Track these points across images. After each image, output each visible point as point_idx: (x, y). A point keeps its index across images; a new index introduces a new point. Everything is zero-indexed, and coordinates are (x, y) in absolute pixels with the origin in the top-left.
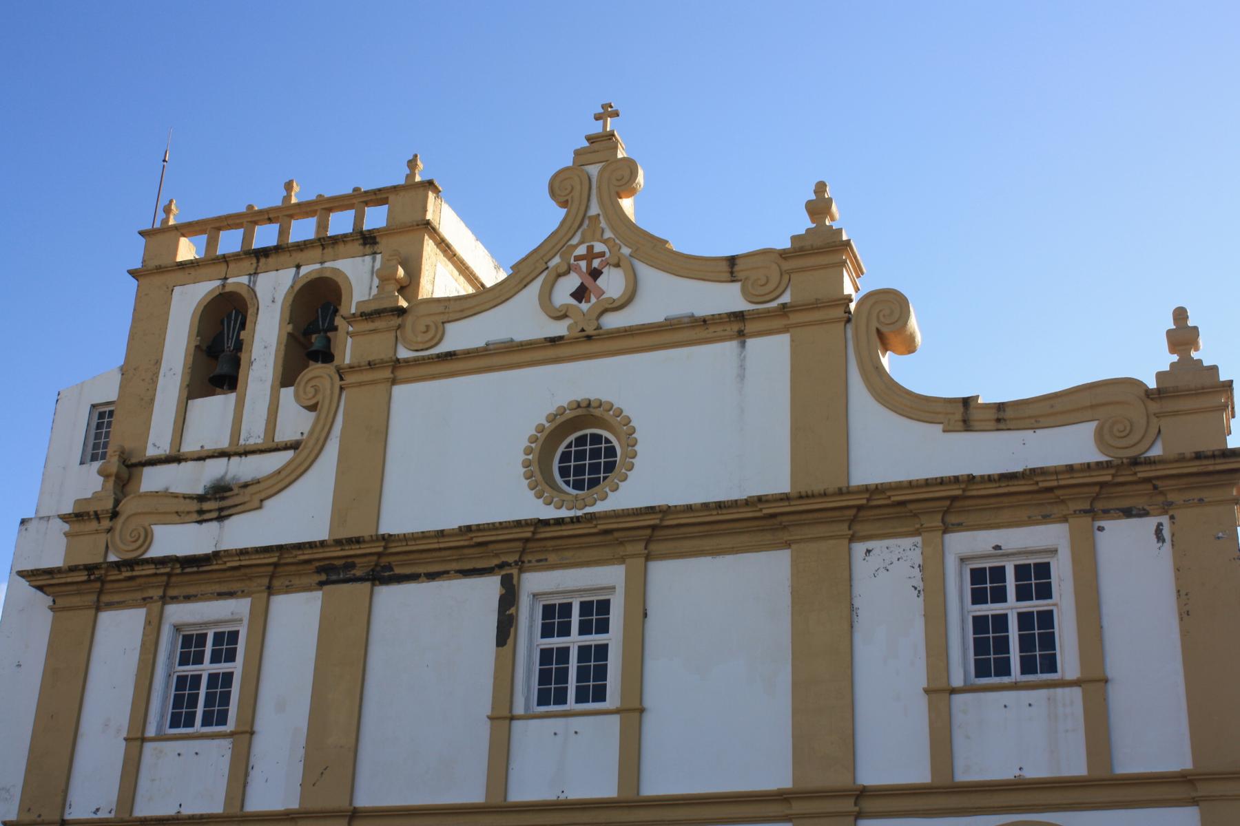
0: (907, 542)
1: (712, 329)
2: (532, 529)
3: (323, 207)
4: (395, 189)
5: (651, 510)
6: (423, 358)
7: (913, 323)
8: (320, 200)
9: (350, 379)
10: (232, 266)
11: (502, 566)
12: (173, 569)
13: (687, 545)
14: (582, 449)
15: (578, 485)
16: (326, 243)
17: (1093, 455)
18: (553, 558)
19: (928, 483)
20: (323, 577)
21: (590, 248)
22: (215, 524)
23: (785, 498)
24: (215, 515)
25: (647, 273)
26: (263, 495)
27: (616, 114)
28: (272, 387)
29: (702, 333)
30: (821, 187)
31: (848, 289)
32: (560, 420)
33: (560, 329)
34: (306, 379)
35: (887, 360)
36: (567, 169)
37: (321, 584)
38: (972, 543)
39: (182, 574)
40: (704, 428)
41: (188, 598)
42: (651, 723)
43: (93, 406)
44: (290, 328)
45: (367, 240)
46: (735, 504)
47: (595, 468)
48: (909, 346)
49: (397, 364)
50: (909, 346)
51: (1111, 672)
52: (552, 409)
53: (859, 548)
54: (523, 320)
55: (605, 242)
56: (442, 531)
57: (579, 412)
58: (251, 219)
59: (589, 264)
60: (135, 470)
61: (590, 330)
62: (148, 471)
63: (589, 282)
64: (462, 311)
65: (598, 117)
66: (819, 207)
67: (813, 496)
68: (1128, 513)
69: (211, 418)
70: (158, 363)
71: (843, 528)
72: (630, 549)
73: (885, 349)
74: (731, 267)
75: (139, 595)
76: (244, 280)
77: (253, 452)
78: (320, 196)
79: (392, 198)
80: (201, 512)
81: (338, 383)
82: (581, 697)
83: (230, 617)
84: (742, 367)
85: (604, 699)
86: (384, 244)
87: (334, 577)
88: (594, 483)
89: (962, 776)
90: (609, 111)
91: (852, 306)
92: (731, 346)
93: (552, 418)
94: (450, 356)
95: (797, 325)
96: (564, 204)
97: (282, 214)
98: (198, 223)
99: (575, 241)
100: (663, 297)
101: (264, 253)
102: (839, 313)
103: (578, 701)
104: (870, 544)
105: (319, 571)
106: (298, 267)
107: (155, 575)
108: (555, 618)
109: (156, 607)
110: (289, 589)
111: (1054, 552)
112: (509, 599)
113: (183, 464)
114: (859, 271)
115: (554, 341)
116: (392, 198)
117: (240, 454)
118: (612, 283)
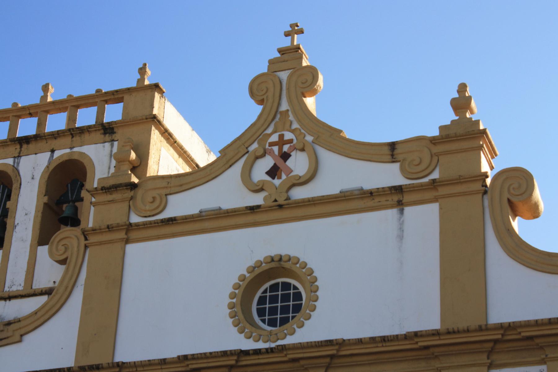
1: (377, 200)
2: (235, 358)
3: (72, 105)
4: (129, 90)
5: (329, 343)
6: (151, 223)
7: (537, 194)
9: (93, 239)
15: (272, 323)
16: (74, 133)
21: (281, 136)
23: (435, 333)
25: (325, 155)
26: (22, 331)
27: (301, 32)
29: (369, 203)
30: (462, 88)
31: (485, 167)
32: (257, 271)
33: (258, 199)
34: (57, 240)
35: (516, 224)
36: (263, 75)
44: (46, 199)
45: (107, 130)
46: (396, 338)
47: (285, 310)
48: (534, 212)
49: (130, 227)
50: (534, 212)
52: (251, 263)
54: (228, 192)
55: (293, 131)
56: (164, 360)
57: (273, 265)
59: (280, 149)
61: (281, 201)
63: (280, 162)
64: (181, 185)
65: (287, 34)
66: (461, 104)
67: (459, 332)
71: (483, 358)
73: (515, 215)
74: (392, 151)
77: (16, 297)
78: (70, 96)
79: (126, 97)
81: (83, 242)
84: (401, 229)
86: (119, 134)
88: (285, 321)
90: (295, 30)
91: (488, 181)
92: (392, 213)
94: (171, 221)
96: (260, 102)
97: (40, 110)
99: (269, 131)
100: (339, 175)
101: (26, 140)
102: (477, 186)
106: (53, 151)
114: (493, 153)
115: (253, 209)
116: (126, 97)
118: (298, 164)
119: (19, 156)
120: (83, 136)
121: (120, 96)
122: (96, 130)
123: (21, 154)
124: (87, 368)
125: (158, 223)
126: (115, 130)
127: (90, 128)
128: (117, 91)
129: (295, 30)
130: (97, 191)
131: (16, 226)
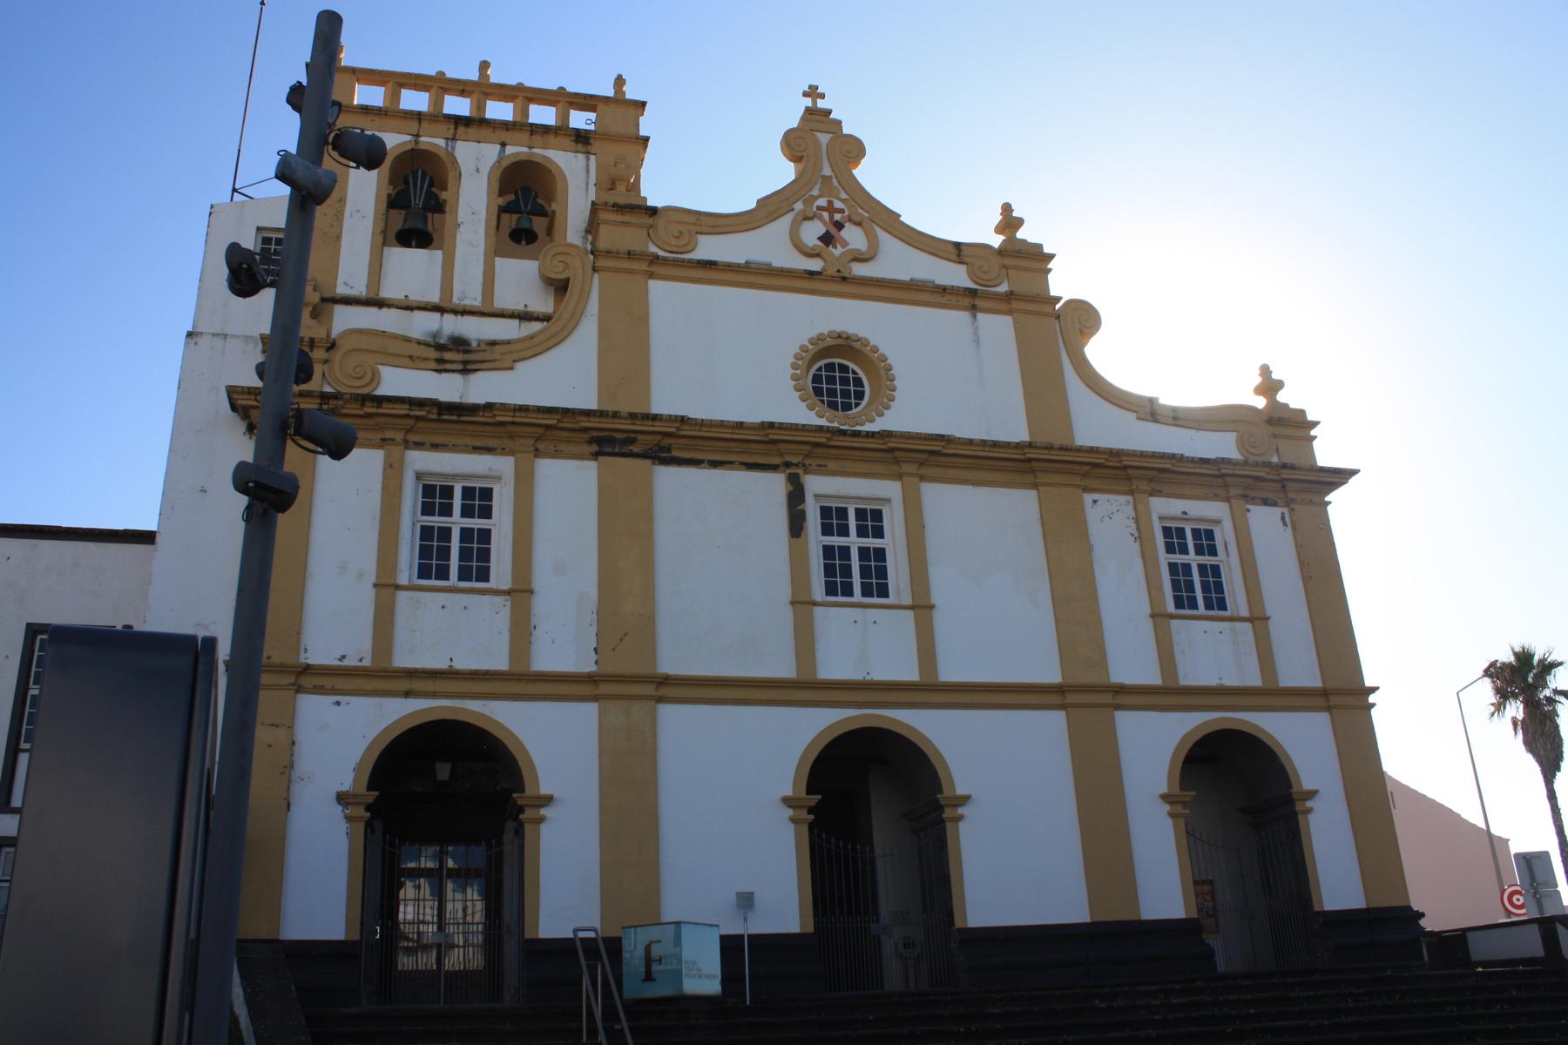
0: (1123, 499)
1: (948, 297)
3: (523, 95)
6: (675, 260)
8: (520, 88)
10: (425, 125)
11: (788, 465)
13: (952, 473)
14: (838, 372)
17: (1235, 455)
18: (831, 465)
19: (1154, 455)
20: (595, 448)
21: (831, 203)
22: (457, 377)
24: (460, 367)
25: (882, 235)
26: (515, 356)
27: (822, 96)
29: (938, 298)
30: (1007, 209)
32: (822, 345)
33: (815, 265)
34: (553, 252)
37: (595, 456)
38: (1165, 507)
39: (438, 421)
40: (944, 378)
41: (435, 447)
42: (940, 619)
43: (259, 229)
45: (582, 139)
46: (1007, 445)
49: (655, 259)
51: (934, 601)
52: (814, 333)
53: (1088, 498)
54: (771, 246)
55: (843, 201)
57: (839, 341)
58: (440, 85)
59: (831, 217)
60: (328, 306)
61: (845, 274)
62: (340, 311)
63: (833, 231)
65: (805, 94)
68: (1265, 502)
69: (412, 271)
72: (906, 468)
74: (958, 252)
75: (379, 436)
76: (441, 142)
79: (601, 107)
80: (440, 361)
82: (867, 592)
83: (486, 472)
84: (976, 334)
85: (487, 580)
86: (596, 146)
87: (608, 450)
89: (1184, 681)
90: (813, 92)
92: (964, 316)
93: (811, 341)
94: (710, 265)
95: (1019, 311)
96: (796, 159)
97: (482, 89)
98: (381, 73)
99: (815, 192)
100: (896, 263)
101: (458, 121)
103: (461, 579)
104: (1096, 496)
105: (590, 442)
106: (503, 145)
107: (408, 416)
108: (833, 519)
110: (556, 455)
111: (1218, 522)
112: (796, 497)
113: (385, 310)
115: (811, 274)
116: (601, 107)
117: (455, 312)
118: (853, 237)
128: (591, 96)
129: (813, 92)
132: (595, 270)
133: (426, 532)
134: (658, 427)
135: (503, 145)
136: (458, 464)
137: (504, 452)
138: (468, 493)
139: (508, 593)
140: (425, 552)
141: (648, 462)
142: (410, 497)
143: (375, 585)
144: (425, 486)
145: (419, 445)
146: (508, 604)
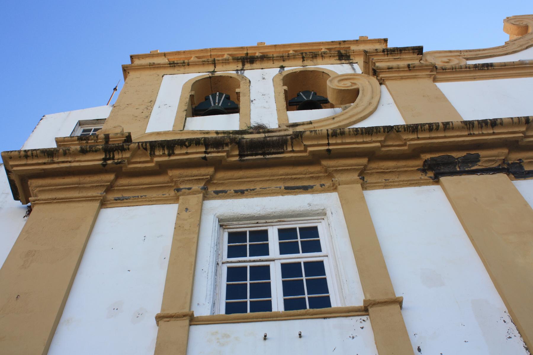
12: (228, 156)
20: (431, 174)
28: (278, 110)
37: (436, 180)
41: (240, 193)
70: (152, 102)
105: (424, 171)
106: (282, 67)
109: (194, 200)
119: (242, 70)
120: (315, 60)
121: (347, 46)
122: (331, 56)
123: (245, 68)
124: (476, 123)
125: (469, 68)
126: (351, 58)
127: (324, 54)
128: (344, 41)
130: (377, 52)
131: (252, 101)
132: (381, 84)
133: (235, 273)
134: (502, 134)
135: (282, 67)
136: (269, 205)
137: (323, 189)
138: (283, 233)
139: (364, 310)
140: (233, 291)
141: (502, 177)
142: (211, 247)
143: (159, 318)
144: (231, 235)
145: (220, 194)
146: (367, 324)
